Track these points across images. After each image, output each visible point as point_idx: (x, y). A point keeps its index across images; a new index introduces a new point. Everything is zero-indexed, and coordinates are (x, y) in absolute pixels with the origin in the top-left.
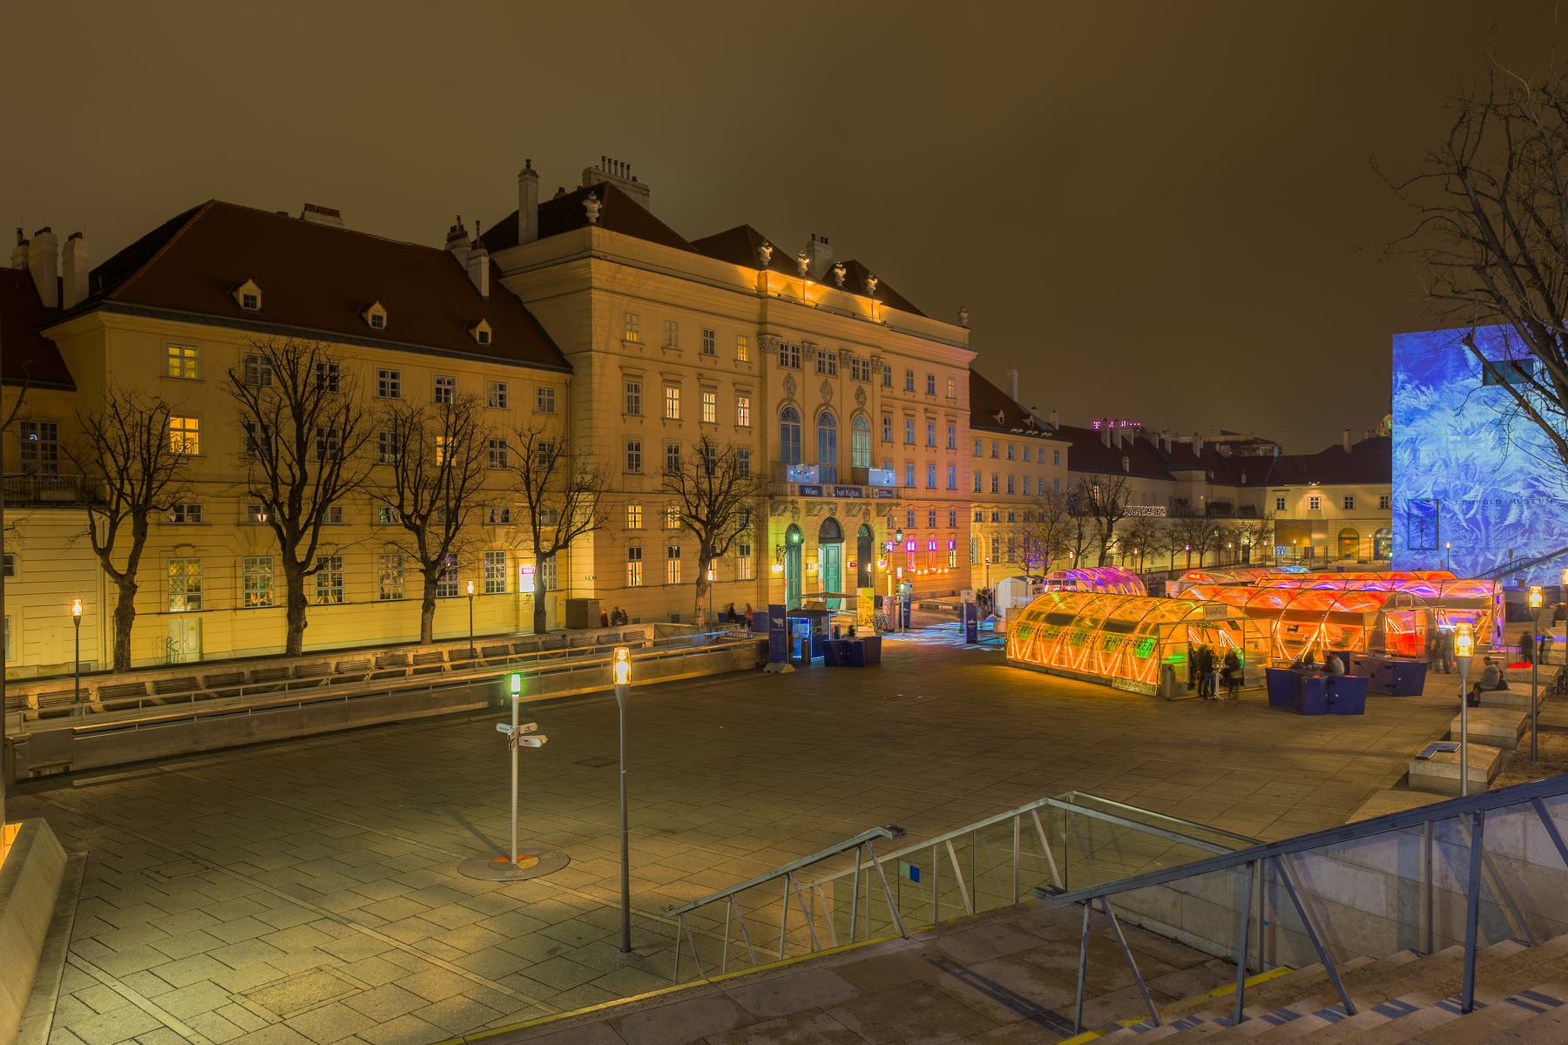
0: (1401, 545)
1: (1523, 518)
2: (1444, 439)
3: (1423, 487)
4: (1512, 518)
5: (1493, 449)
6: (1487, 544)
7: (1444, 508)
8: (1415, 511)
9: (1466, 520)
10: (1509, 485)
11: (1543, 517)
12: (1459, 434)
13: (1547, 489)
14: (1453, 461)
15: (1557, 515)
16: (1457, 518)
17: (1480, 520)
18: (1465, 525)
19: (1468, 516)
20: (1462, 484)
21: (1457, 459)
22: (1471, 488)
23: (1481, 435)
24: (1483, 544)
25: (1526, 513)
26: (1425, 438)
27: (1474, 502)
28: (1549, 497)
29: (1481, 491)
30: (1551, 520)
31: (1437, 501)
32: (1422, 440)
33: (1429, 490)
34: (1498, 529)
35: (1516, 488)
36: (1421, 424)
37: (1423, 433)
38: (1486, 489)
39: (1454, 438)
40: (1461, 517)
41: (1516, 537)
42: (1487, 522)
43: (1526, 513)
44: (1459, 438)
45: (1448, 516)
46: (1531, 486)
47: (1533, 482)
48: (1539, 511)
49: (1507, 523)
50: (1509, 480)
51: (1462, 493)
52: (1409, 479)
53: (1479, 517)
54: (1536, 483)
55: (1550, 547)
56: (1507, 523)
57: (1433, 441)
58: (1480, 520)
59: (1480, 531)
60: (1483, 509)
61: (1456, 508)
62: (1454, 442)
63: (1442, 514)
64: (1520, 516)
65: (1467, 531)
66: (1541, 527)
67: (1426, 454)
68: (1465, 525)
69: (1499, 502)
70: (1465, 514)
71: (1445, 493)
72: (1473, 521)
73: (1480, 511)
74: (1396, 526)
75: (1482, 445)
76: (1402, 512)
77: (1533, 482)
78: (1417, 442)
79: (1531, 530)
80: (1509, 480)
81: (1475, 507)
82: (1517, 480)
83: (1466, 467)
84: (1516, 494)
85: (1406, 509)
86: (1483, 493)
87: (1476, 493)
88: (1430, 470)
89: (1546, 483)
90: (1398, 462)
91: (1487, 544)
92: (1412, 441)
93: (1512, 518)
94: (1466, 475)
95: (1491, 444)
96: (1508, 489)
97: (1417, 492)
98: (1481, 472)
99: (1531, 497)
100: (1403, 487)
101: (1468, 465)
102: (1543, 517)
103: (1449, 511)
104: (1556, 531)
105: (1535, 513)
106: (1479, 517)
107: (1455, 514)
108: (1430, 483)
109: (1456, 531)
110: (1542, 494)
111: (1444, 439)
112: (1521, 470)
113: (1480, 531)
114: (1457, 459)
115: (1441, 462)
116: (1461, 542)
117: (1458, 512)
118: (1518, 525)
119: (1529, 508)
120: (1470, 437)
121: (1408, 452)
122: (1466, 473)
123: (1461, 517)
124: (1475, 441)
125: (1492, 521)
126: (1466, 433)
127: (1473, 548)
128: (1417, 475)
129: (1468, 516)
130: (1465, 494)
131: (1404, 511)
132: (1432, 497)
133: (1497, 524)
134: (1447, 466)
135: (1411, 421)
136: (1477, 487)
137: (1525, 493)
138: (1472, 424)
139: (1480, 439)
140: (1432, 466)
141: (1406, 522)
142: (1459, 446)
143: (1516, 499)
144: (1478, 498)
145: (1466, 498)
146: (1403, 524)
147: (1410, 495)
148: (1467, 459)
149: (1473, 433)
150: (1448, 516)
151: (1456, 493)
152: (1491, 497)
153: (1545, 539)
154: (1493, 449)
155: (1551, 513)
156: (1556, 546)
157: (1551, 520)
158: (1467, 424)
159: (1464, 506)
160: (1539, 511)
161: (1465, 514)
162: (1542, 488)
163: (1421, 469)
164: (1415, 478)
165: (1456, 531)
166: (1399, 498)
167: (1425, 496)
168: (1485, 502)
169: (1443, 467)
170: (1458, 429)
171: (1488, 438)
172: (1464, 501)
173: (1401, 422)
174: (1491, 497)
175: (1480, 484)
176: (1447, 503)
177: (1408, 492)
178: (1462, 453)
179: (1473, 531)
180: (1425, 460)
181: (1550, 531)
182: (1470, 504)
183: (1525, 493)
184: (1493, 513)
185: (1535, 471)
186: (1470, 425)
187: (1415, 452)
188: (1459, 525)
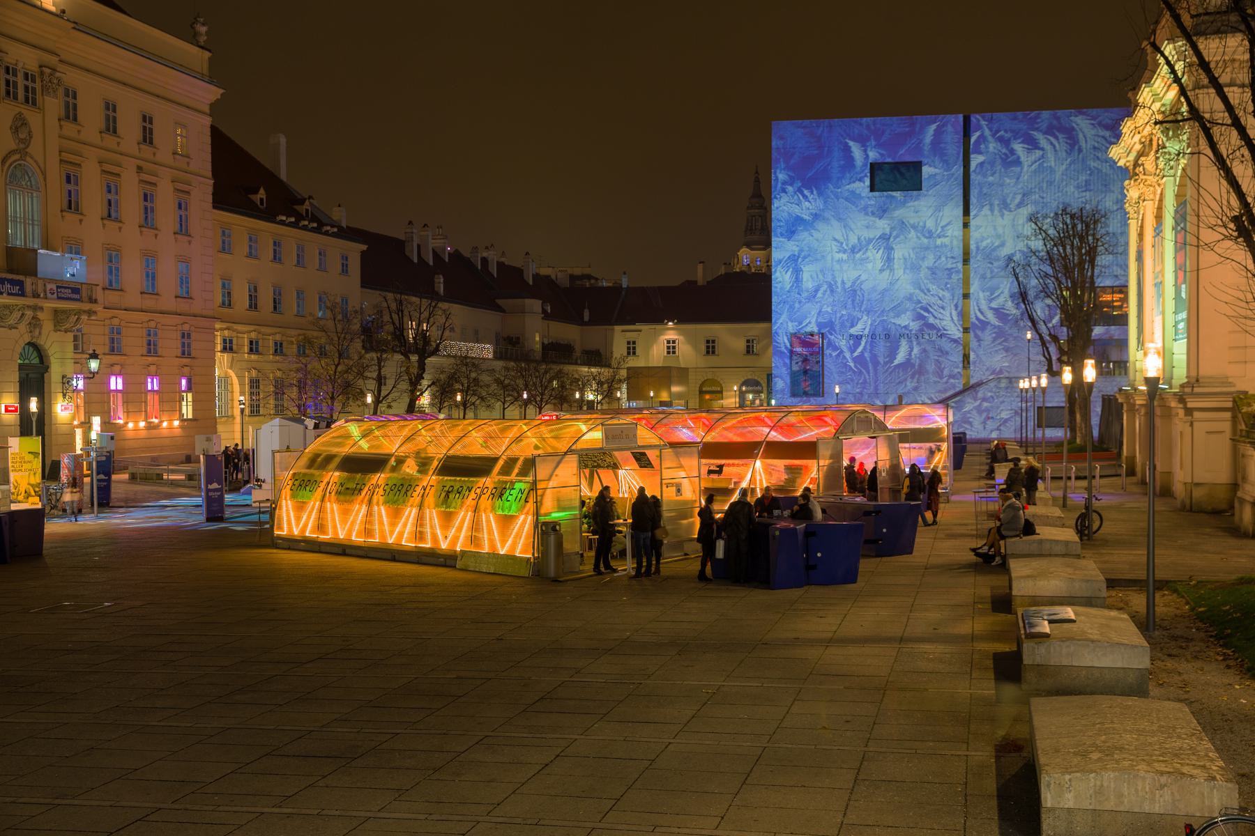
0: (782, 391)
3: (806, 317)
5: (881, 271)
6: (876, 388)
7: (830, 344)
8: (799, 349)
9: (855, 360)
12: (845, 251)
14: (839, 284)
21: (843, 282)
22: (859, 319)
23: (869, 254)
24: (871, 389)
26: (809, 255)
29: (869, 323)
32: (805, 258)
33: (814, 321)
36: (804, 236)
39: (841, 255)
40: (848, 355)
44: (845, 257)
45: (834, 354)
50: (898, 310)
51: (848, 325)
52: (792, 307)
57: (817, 260)
61: (843, 344)
62: (840, 261)
63: (827, 352)
71: (830, 324)
72: (860, 360)
74: (776, 367)
75: (870, 266)
76: (783, 349)
78: (800, 260)
80: (898, 310)
82: (907, 310)
83: (854, 293)
85: (788, 345)
87: (863, 326)
88: (815, 296)
95: (879, 265)
96: (898, 321)
97: (800, 323)
98: (868, 300)
100: (784, 317)
101: (855, 291)
103: (835, 348)
111: (829, 258)
114: (843, 282)
115: (825, 287)
116: (849, 387)
120: (858, 256)
121: (789, 273)
123: (848, 355)
126: (854, 250)
127: (861, 393)
128: (800, 302)
130: (852, 326)
131: (786, 348)
132: (816, 330)
134: (832, 291)
136: (865, 318)
138: (859, 239)
140: (817, 291)
141: (788, 361)
142: (845, 267)
145: (853, 331)
146: (785, 364)
147: (792, 327)
148: (854, 283)
149: (860, 250)
150: (834, 354)
151: (842, 325)
154: (881, 271)
158: (853, 240)
163: (805, 295)
164: (797, 305)
166: (780, 332)
167: (808, 329)
169: (828, 292)
170: (844, 245)
172: (851, 335)
175: (868, 315)
178: (848, 274)
180: (808, 283)
187: (797, 272)
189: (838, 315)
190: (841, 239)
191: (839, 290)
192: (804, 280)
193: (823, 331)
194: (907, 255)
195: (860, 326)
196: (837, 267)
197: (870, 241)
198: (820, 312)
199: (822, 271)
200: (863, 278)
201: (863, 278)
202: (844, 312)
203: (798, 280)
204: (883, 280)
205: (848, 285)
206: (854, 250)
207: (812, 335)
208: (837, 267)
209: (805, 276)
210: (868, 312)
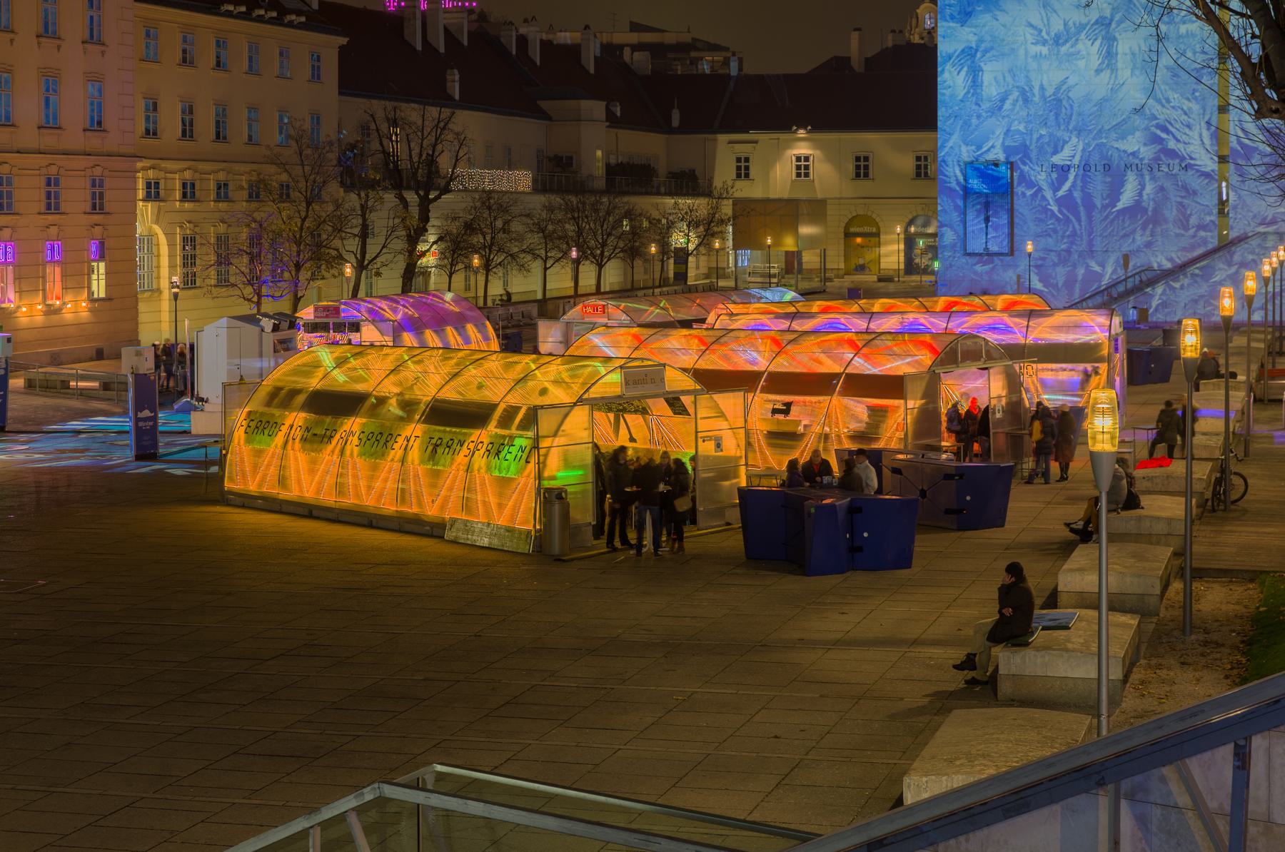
0: (953, 246)
1: (1145, 197)
2: (1022, 52)
3: (988, 139)
4: (1126, 199)
5: (1098, 71)
6: (1091, 244)
7: (1023, 178)
8: (975, 183)
9: (1059, 201)
10: (1123, 137)
11: (1174, 196)
12: (1044, 43)
13: (1180, 146)
14: (1036, 91)
15: (1195, 193)
16: (1044, 198)
17: (1079, 201)
18: (1055, 208)
19: (1061, 193)
20: (1051, 135)
21: (1042, 88)
22: (1065, 142)
23: (1080, 46)
25: (1149, 189)
26: (992, 48)
27: (1069, 167)
28: (1182, 159)
29: (1081, 147)
30: (1186, 201)
31: (1012, 166)
32: (986, 51)
33: (998, 144)
34: (1107, 217)
35: (1133, 144)
37: (988, 38)
38: (1088, 145)
40: (1048, 194)
41: (1134, 231)
42: (1089, 206)
43: (1149, 189)
44: (1045, 50)
45: (1029, 193)
46: (1156, 140)
47: (1158, 132)
48: (1168, 184)
49: (1120, 206)
51: (1049, 150)
52: (967, 124)
53: (1077, 195)
54: (1164, 135)
55: (1184, 249)
56: (1120, 206)
57: (1003, 55)
58: (1079, 201)
59: (1079, 221)
60: (1083, 181)
61: (1041, 178)
62: (1038, 57)
63: (1019, 190)
64: (1140, 195)
65: (1058, 219)
66: (1171, 213)
67: (991, 73)
68: (1055, 208)
69: (1107, 168)
70: (1056, 189)
71: (1024, 150)
73: (1079, 183)
74: (944, 211)
75: (1082, 64)
76: (954, 185)
77: (1158, 132)
78: (979, 55)
79: (1156, 219)
80: (1122, 130)
81: (1071, 177)
83: (1057, 104)
84: (1133, 154)
85: (961, 178)
86: (1084, 150)
88: (1000, 108)
89: (1178, 135)
90: (947, 92)
91: (1091, 244)
92: (970, 54)
93: (1126, 199)
94: (1057, 119)
95: (1095, 62)
96: (1122, 145)
97: (979, 148)
98: (1080, 114)
99: (1157, 159)
100: (955, 139)
101: (1060, 101)
102: (1174, 196)
103: (1030, 184)
104: (1193, 221)
105: (1162, 189)
106: (1077, 195)
107: (1040, 189)
108: (1000, 131)
109: (1040, 220)
110: (1172, 154)
111: (1022, 52)
112: (1138, 111)
113: (1079, 221)
114: (1042, 88)
115: (1016, 94)
117: (1045, 186)
118: (1136, 209)
119: (1153, 179)
120: (1064, 49)
121: (963, 73)
122: (1057, 115)
123: (1048, 194)
124: (1072, 56)
125: (1098, 203)
126: (1058, 41)
127: (1068, 251)
128: (979, 117)
129: (1061, 193)
130: (1055, 152)
131: (958, 183)
132: (1002, 157)
133: (1105, 207)
135: (969, 14)
136: (1074, 140)
137: (1147, 152)
138: (1065, 25)
139: (1079, 52)
140: (1003, 100)
141: (960, 203)
143: (1132, 163)
144: (1076, 161)
145: (1057, 159)
146: (956, 207)
147: (966, 153)
148: (1058, 88)
149: (1067, 41)
150: (1029, 193)
151: (1041, 150)
152: (1095, 158)
153: (1177, 235)
154: (1098, 71)
155: (1185, 188)
156: (1192, 248)
157: (1186, 201)
158: (1057, 26)
159: (1054, 175)
160: (1168, 184)
161: (1056, 189)
162: (1172, 144)
163: (986, 105)
164: (974, 121)
165: (1040, 220)
166: (949, 159)
167: (991, 157)
168: (1086, 167)
169: (1020, 102)
170: (1044, 33)
171: (1090, 50)
172: (1054, 166)
173: (952, 17)
174: (1095, 158)
175: (1078, 136)
176: (1026, 168)
177: (964, 149)
178: (1049, 77)
179: (1068, 220)
180: (990, 88)
181: (1184, 223)
182: (1064, 170)
183: (1147, 152)
184: (1098, 186)
185: (1162, 113)
186: (1062, 28)
187: (975, 72)
188: (1046, 210)
189: (1035, 136)
190: (1041, 26)
191: (1036, 99)
192: (985, 84)
193: (1012, 159)
194: (1136, 49)
195: (1067, 152)
196: (1033, 65)
197: (1081, 28)
198: (1008, 130)
199: (1010, 71)
200: (1071, 81)
201: (1071, 81)
202: (1043, 132)
203: (975, 84)
204: (1101, 86)
205: (1050, 91)
206: (1058, 41)
207: (997, 165)
208: (1033, 65)
209: (987, 78)
210: (1079, 132)
